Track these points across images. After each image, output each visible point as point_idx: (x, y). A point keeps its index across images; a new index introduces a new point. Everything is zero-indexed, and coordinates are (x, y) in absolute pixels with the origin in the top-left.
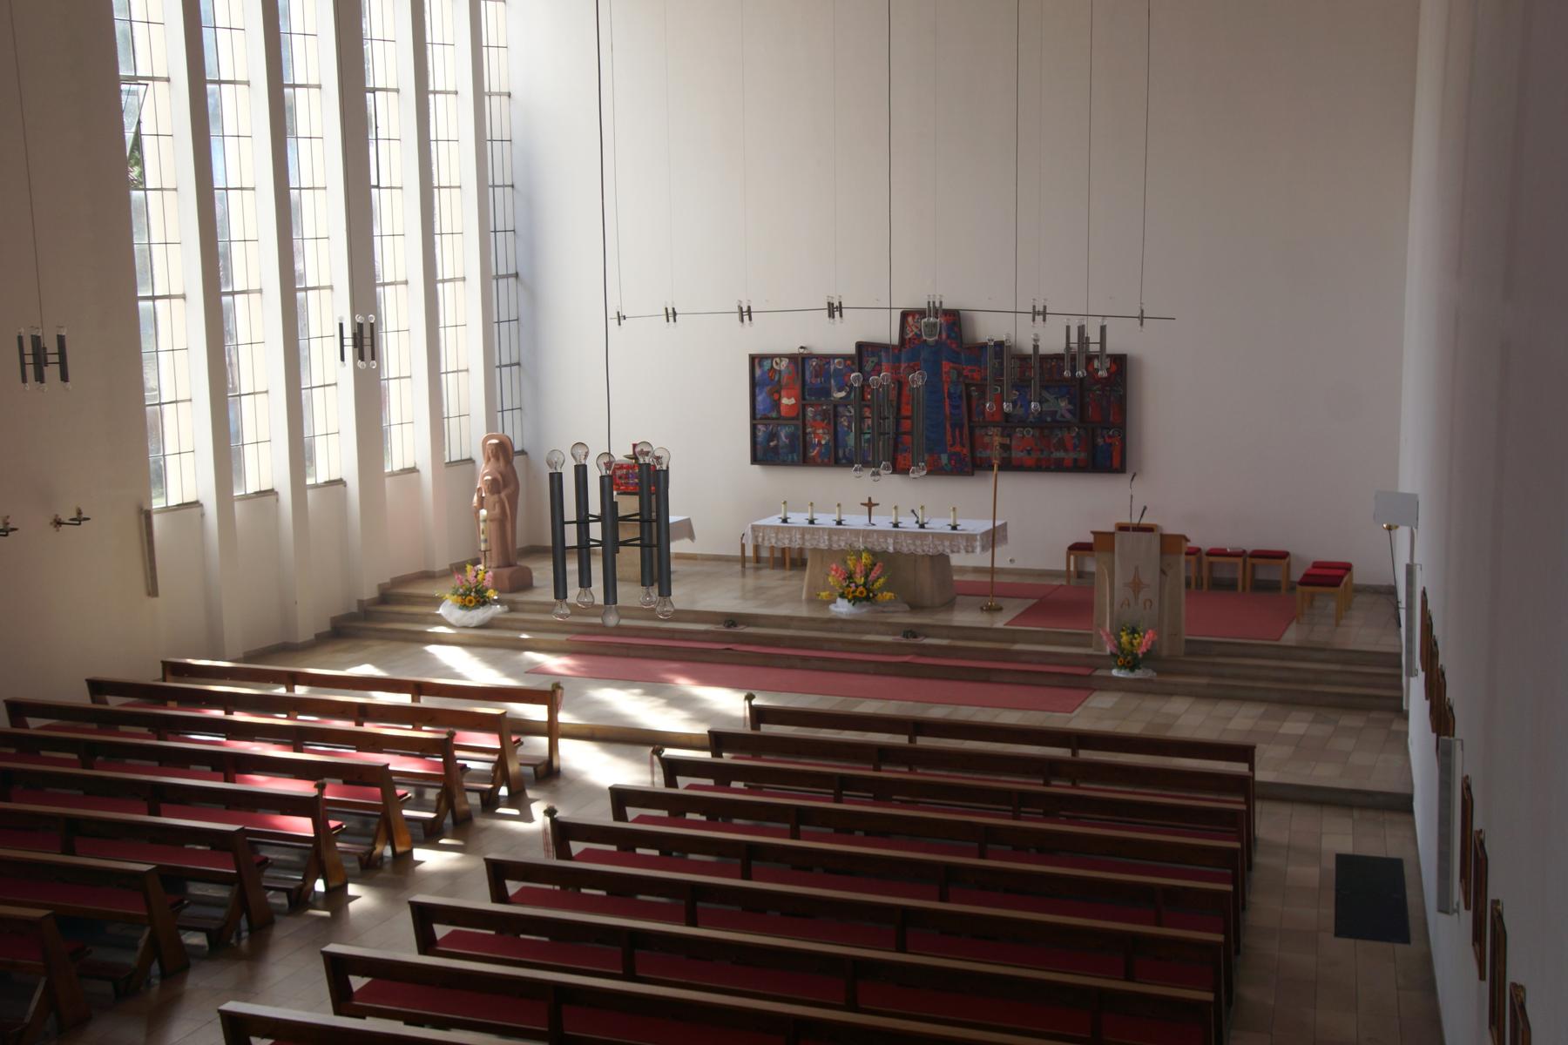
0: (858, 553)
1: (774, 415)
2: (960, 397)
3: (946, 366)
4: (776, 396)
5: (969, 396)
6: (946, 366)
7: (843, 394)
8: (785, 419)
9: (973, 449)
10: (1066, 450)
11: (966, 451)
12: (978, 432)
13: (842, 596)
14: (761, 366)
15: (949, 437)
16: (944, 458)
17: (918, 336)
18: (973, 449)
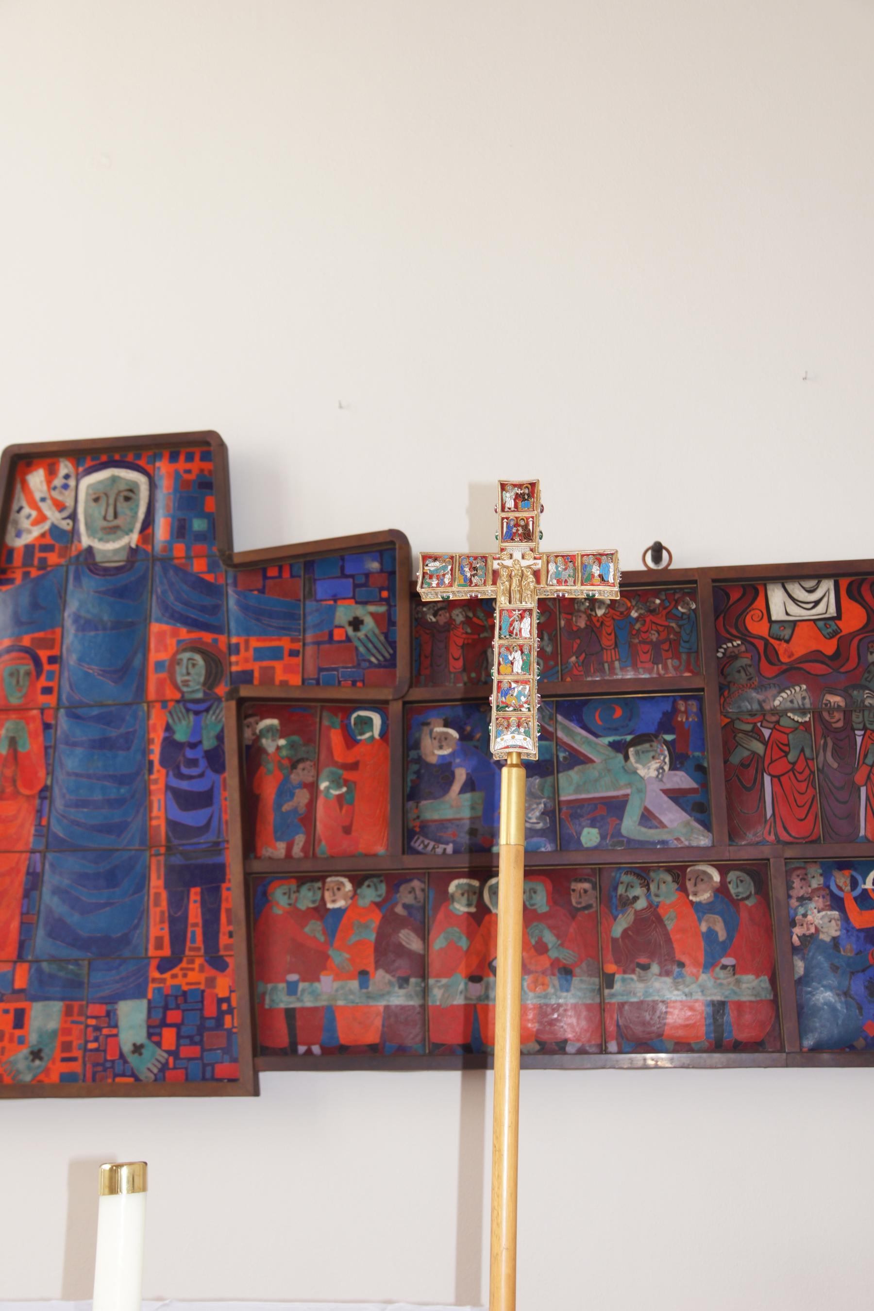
2: (215, 758)
3: (163, 639)
5: (251, 756)
6: (163, 639)
9: (258, 969)
11: (228, 985)
12: (281, 898)
15: (157, 928)
16: (132, 1019)
17: (63, 537)
18: (258, 969)
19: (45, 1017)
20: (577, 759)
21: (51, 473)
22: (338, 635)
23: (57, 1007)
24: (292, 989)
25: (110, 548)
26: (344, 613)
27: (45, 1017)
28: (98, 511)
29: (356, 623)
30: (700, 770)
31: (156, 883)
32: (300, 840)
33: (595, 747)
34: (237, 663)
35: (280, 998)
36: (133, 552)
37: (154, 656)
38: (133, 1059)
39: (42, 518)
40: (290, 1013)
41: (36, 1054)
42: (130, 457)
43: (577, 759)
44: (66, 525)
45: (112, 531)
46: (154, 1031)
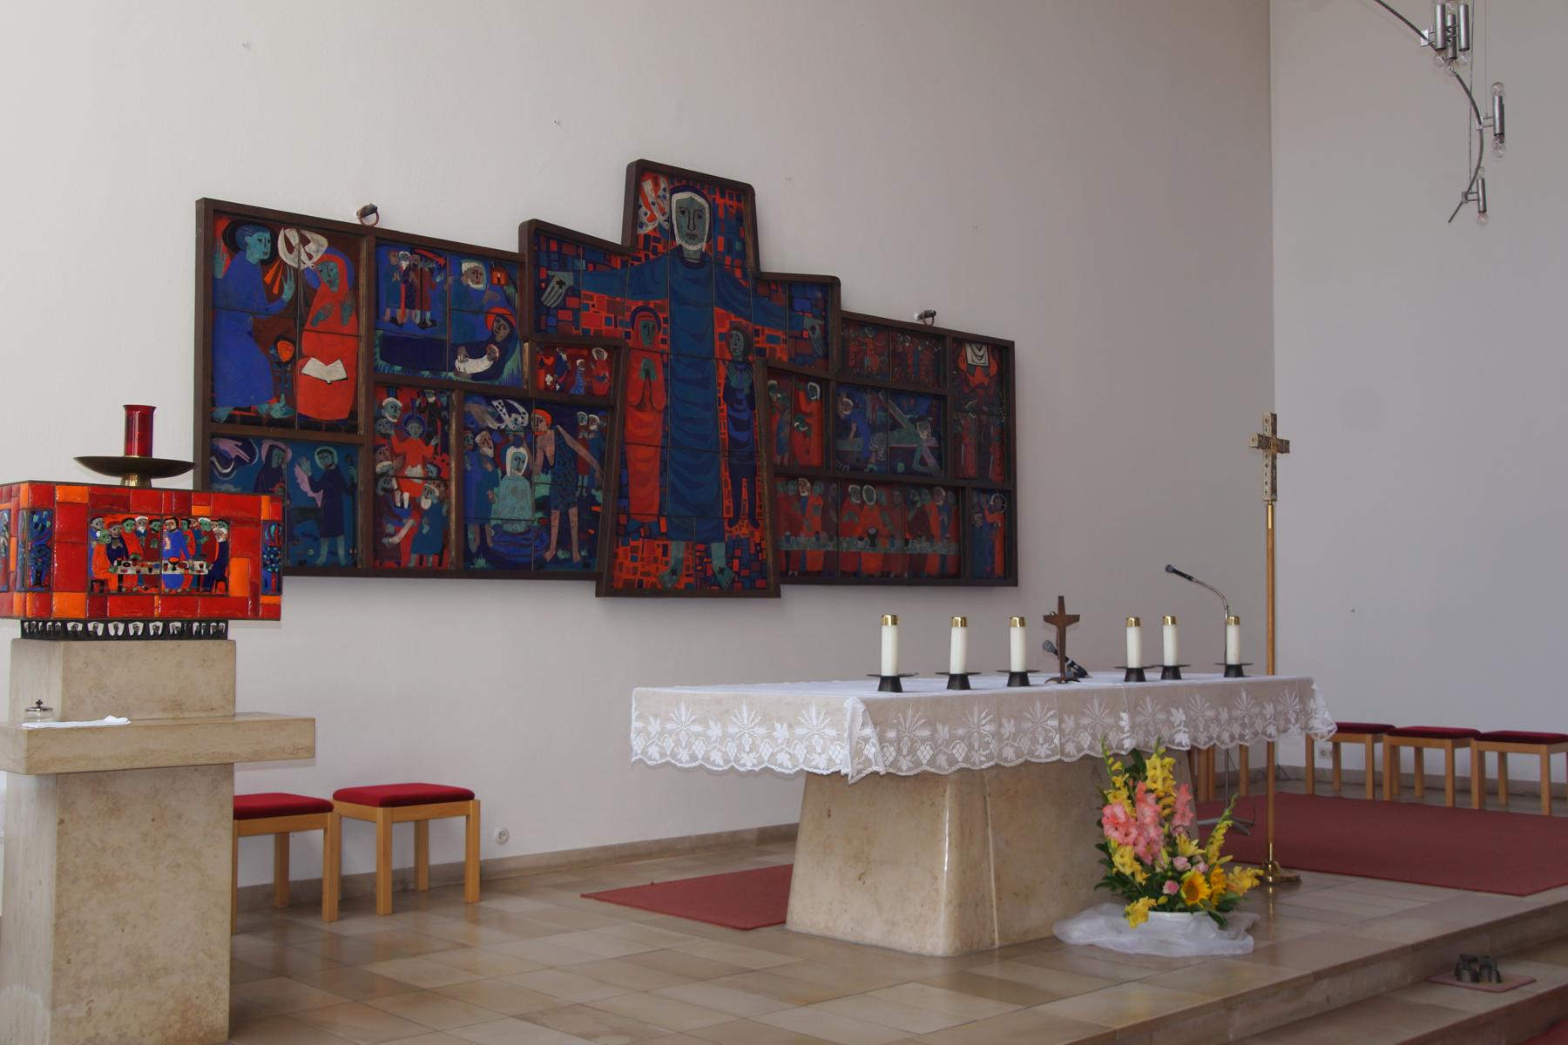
0: (1136, 764)
1: (277, 410)
4: (285, 351)
7: (481, 365)
8: (309, 424)
10: (930, 538)
13: (1172, 905)
14: (235, 247)
15: (728, 503)
16: (718, 551)
19: (677, 550)
20: (895, 426)
21: (656, 185)
22: (805, 334)
23: (682, 544)
24: (788, 541)
25: (693, 249)
26: (808, 321)
27: (677, 550)
28: (685, 222)
29: (813, 329)
30: (939, 439)
31: (725, 474)
32: (787, 455)
33: (903, 418)
34: (760, 342)
35: (785, 547)
36: (703, 255)
37: (719, 330)
38: (719, 576)
39: (652, 218)
40: (787, 553)
41: (674, 572)
42: (698, 186)
43: (895, 426)
44: (666, 225)
45: (692, 237)
46: (730, 558)
